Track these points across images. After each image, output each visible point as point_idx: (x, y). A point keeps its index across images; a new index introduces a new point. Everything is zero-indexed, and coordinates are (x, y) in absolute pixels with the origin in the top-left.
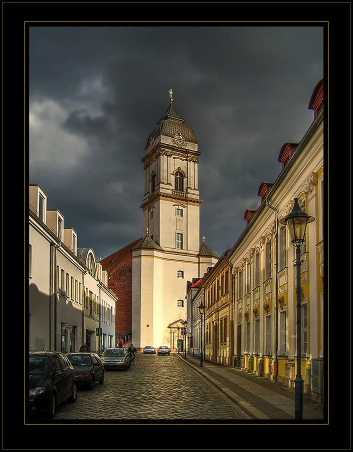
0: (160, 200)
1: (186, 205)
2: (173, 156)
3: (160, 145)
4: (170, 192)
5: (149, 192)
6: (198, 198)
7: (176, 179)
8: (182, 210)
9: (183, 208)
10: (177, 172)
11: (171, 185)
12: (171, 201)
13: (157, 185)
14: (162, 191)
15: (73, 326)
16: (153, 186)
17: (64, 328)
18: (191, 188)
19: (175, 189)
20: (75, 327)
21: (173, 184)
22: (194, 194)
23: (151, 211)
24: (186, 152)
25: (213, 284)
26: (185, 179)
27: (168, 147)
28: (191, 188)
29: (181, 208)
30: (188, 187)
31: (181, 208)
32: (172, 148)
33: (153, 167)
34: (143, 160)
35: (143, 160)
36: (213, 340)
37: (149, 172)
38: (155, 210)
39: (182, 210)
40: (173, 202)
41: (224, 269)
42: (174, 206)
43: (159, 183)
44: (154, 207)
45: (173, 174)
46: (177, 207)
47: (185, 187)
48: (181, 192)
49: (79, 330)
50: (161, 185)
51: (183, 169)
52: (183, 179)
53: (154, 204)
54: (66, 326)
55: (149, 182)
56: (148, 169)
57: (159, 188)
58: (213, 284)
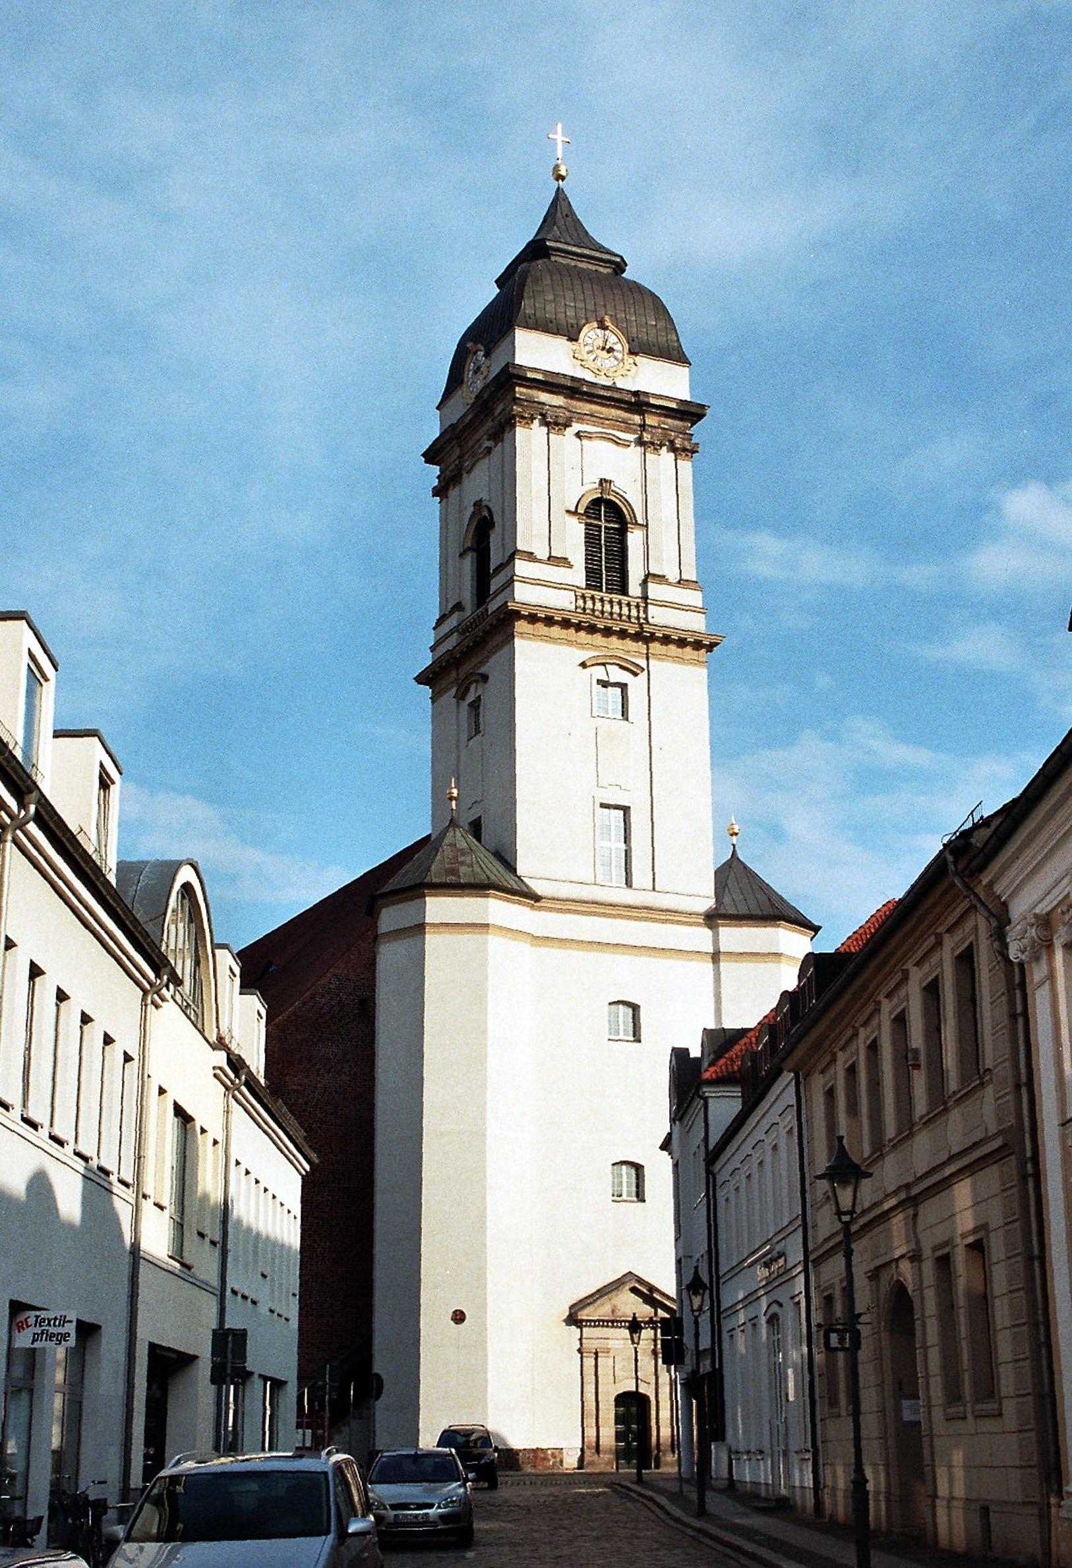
0: (517, 641)
1: (643, 663)
2: (576, 427)
3: (512, 376)
5: (458, 607)
6: (696, 623)
7: (591, 540)
8: (623, 687)
9: (624, 677)
10: (596, 503)
11: (563, 562)
12: (570, 643)
13: (500, 568)
14: (524, 594)
15: (78, 1321)
16: (483, 576)
17: (23, 1340)
19: (588, 587)
20: (87, 1331)
21: (578, 556)
23: (471, 697)
24: (638, 403)
25: (861, 1044)
26: (634, 539)
27: (552, 384)
28: (661, 579)
29: (617, 675)
30: (648, 577)
31: (617, 675)
32: (573, 389)
33: (476, 485)
34: (431, 456)
35: (431, 456)
36: (927, 1377)
38: (489, 693)
39: (623, 687)
40: (582, 646)
41: (939, 943)
42: (583, 665)
43: (512, 558)
44: (485, 678)
45: (575, 513)
46: (599, 673)
47: (635, 573)
48: (616, 597)
49: (111, 1345)
50: (521, 567)
51: (628, 489)
52: (623, 532)
53: (482, 663)
54: (39, 1322)
56: (453, 493)
57: (511, 582)
58: (861, 1044)
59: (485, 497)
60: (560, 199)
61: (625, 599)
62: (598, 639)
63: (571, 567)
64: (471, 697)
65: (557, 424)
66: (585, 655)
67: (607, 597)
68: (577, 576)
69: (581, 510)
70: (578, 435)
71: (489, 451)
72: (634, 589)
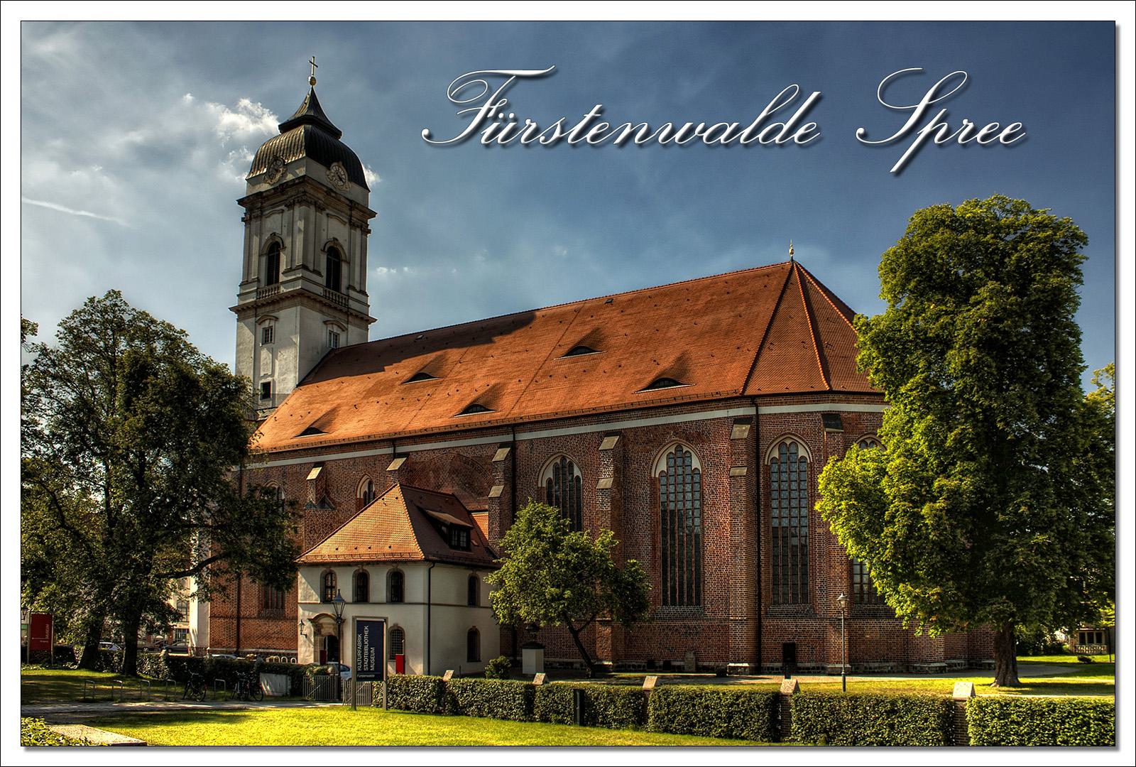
0: (295, 308)
2: (327, 211)
4: (319, 291)
8: (336, 336)
9: (339, 331)
11: (319, 274)
18: (354, 289)
21: (324, 273)
22: (315, 283)
23: (266, 324)
26: (344, 268)
28: (354, 289)
29: (336, 329)
31: (336, 329)
37: (260, 234)
46: (330, 328)
47: (344, 283)
55: (260, 255)
59: (278, 231)
60: (313, 96)
61: (338, 293)
62: (330, 311)
63: (322, 277)
64: (266, 324)
65: (319, 208)
66: (327, 318)
67: (331, 291)
68: (323, 280)
69: (326, 250)
70: (327, 215)
71: (283, 211)
72: (343, 290)
